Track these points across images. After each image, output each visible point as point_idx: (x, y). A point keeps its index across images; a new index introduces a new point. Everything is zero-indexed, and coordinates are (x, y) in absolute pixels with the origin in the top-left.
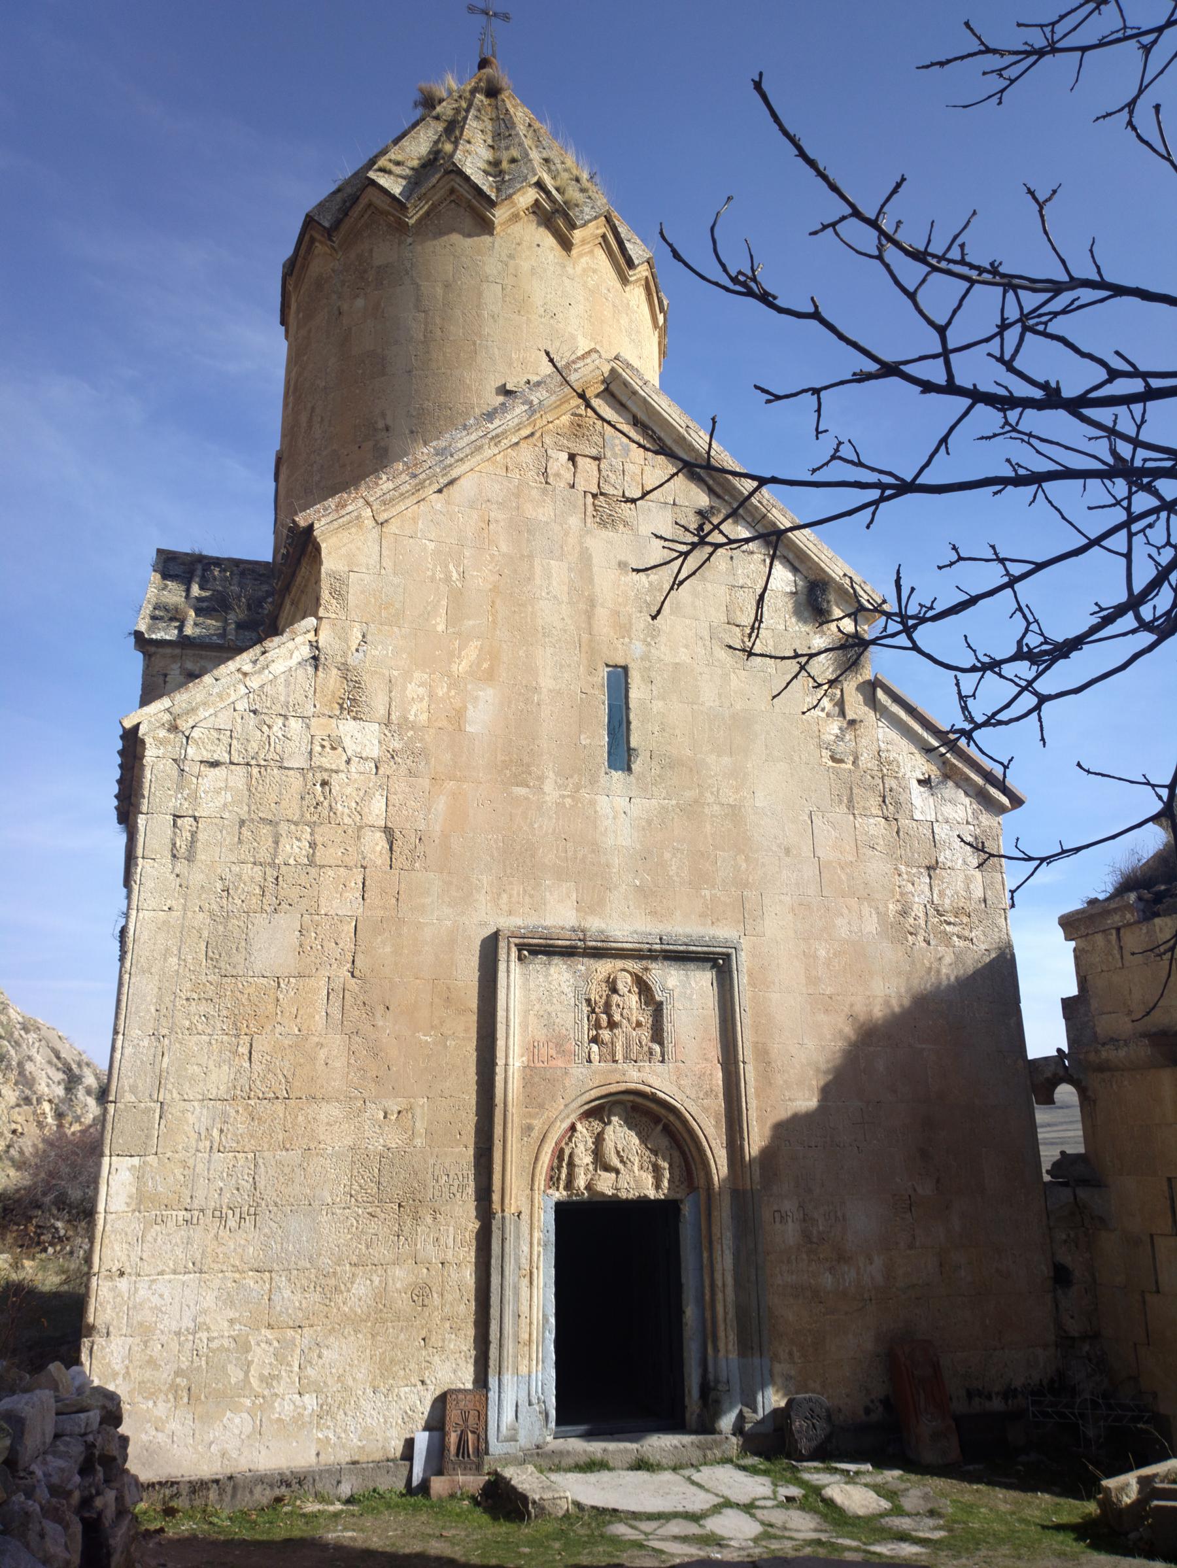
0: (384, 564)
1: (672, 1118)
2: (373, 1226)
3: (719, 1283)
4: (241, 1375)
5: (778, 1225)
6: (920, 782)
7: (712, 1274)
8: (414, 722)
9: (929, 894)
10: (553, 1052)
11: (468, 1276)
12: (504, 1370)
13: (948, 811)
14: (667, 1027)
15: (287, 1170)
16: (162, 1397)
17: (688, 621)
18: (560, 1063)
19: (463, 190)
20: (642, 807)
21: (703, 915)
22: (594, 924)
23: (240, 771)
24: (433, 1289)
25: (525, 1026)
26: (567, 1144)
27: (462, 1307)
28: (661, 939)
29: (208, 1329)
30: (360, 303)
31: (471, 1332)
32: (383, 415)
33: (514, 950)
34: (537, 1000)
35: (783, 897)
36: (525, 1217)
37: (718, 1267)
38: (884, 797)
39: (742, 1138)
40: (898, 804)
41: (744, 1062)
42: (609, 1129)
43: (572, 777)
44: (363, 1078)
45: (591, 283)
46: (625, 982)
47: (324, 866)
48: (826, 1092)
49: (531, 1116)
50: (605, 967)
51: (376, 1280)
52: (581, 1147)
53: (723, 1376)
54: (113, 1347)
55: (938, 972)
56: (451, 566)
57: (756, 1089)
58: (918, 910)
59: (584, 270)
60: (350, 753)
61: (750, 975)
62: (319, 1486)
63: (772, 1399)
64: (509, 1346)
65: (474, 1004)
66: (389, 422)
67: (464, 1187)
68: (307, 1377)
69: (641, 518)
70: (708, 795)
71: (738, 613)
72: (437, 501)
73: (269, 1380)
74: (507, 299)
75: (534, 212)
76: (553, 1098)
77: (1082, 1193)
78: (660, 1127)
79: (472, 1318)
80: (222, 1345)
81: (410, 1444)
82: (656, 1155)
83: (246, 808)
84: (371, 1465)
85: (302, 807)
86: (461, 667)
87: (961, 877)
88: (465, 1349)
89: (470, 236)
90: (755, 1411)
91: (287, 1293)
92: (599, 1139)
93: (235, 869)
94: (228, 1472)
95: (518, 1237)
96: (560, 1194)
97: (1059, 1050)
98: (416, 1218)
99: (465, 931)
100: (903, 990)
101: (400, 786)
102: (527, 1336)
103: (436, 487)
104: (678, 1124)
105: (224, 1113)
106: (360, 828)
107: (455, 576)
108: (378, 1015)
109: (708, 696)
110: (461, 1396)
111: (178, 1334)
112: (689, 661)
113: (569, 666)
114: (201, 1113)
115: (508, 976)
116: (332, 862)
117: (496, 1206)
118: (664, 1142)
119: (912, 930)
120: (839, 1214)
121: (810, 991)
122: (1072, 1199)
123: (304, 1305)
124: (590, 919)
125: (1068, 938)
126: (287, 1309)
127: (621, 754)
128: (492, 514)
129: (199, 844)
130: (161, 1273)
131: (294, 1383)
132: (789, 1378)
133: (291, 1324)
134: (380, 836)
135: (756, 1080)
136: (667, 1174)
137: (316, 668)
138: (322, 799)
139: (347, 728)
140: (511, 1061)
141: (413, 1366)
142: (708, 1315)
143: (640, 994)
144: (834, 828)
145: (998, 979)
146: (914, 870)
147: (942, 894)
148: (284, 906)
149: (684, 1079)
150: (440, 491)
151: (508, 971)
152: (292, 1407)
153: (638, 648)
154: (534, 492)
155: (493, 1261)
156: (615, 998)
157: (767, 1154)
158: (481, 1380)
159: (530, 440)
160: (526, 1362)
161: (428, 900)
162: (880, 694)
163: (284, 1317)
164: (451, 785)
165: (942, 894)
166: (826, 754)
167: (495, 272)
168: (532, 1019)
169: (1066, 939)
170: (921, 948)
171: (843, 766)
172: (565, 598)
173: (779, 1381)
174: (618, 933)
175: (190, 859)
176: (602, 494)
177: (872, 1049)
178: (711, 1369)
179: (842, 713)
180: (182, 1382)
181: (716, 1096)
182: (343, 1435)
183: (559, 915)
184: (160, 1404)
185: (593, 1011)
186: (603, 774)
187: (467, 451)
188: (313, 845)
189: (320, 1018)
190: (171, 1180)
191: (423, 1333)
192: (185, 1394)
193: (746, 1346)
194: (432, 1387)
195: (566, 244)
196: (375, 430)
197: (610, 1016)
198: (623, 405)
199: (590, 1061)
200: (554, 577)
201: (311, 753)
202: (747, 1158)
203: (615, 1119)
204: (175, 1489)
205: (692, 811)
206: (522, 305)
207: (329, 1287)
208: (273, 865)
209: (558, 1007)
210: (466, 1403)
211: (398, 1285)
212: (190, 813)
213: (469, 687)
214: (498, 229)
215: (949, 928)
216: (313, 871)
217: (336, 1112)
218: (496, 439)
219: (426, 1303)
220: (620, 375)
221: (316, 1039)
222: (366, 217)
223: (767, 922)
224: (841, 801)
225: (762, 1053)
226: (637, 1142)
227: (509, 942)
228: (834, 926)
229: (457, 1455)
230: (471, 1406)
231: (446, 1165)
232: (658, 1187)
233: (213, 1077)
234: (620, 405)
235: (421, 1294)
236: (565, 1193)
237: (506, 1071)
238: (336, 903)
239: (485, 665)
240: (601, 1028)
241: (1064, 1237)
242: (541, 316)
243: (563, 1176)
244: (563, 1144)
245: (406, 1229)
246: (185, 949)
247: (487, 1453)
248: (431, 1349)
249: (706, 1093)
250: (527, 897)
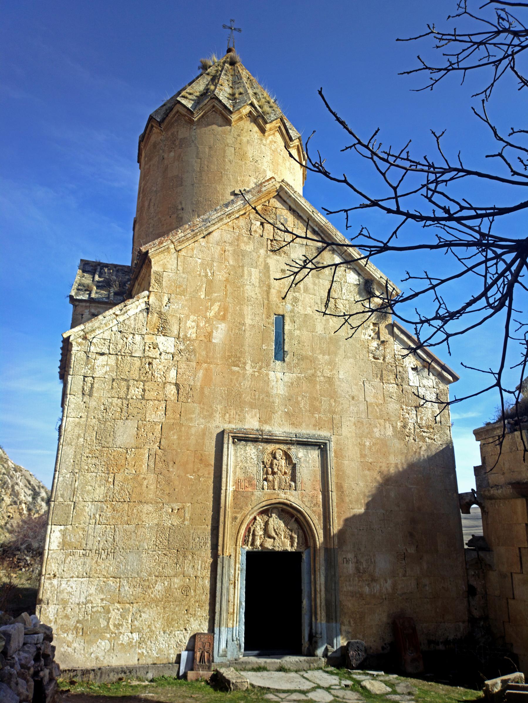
0: (179, 269)
1: (299, 515)
2: (166, 560)
3: (318, 589)
4: (106, 624)
5: (345, 564)
6: (412, 369)
7: (315, 585)
8: (190, 337)
9: (415, 419)
10: (247, 485)
11: (207, 583)
12: (222, 625)
13: (425, 382)
14: (298, 474)
15: (128, 533)
16: (71, 632)
17: (311, 296)
18: (250, 489)
19: (219, 106)
20: (288, 377)
21: (315, 426)
22: (267, 428)
23: (113, 357)
24: (191, 588)
25: (235, 473)
26: (252, 526)
27: (204, 596)
28: (296, 435)
29: (92, 603)
30: (172, 154)
31: (207, 608)
32: (181, 203)
33: (231, 438)
34: (240, 461)
35: (350, 418)
36: (233, 557)
37: (318, 582)
38: (396, 375)
39: (330, 525)
40: (402, 379)
41: (332, 491)
42: (271, 520)
43: (258, 363)
44: (163, 493)
45: (273, 148)
46: (279, 454)
47: (148, 400)
48: (368, 505)
49: (236, 512)
50: (270, 447)
51: (166, 583)
52: (258, 527)
53: (319, 631)
54: (50, 609)
55: (420, 453)
56: (208, 270)
57: (337, 503)
58: (410, 425)
59: (271, 142)
60: (161, 350)
61: (335, 452)
62: (139, 674)
63: (341, 642)
64: (224, 615)
65: (212, 462)
66: (183, 206)
67: (205, 543)
68: (135, 625)
69: (292, 250)
70: (318, 372)
71: (334, 293)
72: (203, 242)
73: (117, 626)
74: (236, 154)
75: (249, 116)
76: (247, 505)
77: (481, 554)
78: (294, 519)
79: (208, 601)
80: (98, 610)
81: (179, 656)
82: (292, 532)
83: (115, 374)
84: (162, 665)
85: (139, 374)
86: (211, 314)
87: (430, 411)
88: (204, 615)
89: (221, 126)
90: (333, 647)
91: (127, 588)
92: (266, 524)
93: (110, 400)
94: (99, 666)
95: (229, 566)
96: (249, 548)
97: (472, 490)
98: (185, 556)
99: (209, 430)
100: (403, 461)
101: (183, 365)
102: (232, 611)
103: (202, 236)
104: (302, 518)
105: (102, 507)
106: (165, 383)
107: (209, 274)
108: (170, 466)
110: (202, 636)
111: (78, 604)
112: (311, 313)
113: (258, 314)
114: (91, 507)
115: (228, 450)
116: (152, 398)
117: (220, 552)
118: (296, 526)
119: (408, 434)
120: (373, 560)
121: (362, 460)
122: (477, 556)
123: (134, 593)
124: (265, 426)
125: (477, 440)
126: (127, 595)
127: (280, 353)
128: (227, 248)
129: (94, 389)
130: (72, 577)
131: (128, 628)
132: (348, 633)
133: (128, 601)
134: (173, 387)
135: (337, 499)
136: (296, 540)
137: (148, 313)
138: (148, 370)
139: (160, 339)
140: (228, 488)
141: (181, 622)
142: (313, 604)
143: (286, 460)
144: (374, 388)
145: (446, 457)
146: (409, 408)
147: (421, 419)
148: (131, 417)
149: (304, 498)
150: (204, 237)
151: (228, 448)
152: (128, 638)
153: (289, 307)
154: (245, 239)
155: (218, 577)
156: (275, 461)
157: (341, 532)
158: (211, 629)
159: (244, 216)
160: (231, 622)
161: (194, 416)
162: (395, 329)
163: (125, 598)
164: (205, 365)
165: (421, 419)
166: (371, 355)
167: (231, 142)
168: (238, 469)
169: (477, 440)
170: (412, 443)
171: (378, 361)
172: (257, 285)
173: (344, 633)
174: (277, 432)
175: (90, 395)
176: (275, 240)
177: (389, 487)
178: (314, 627)
179: (379, 338)
180: (80, 626)
181: (319, 506)
182: (150, 652)
183: (252, 423)
184: (70, 635)
185: (265, 467)
186: (272, 362)
187: (217, 220)
188: (144, 390)
189: (145, 467)
190: (77, 536)
191: (186, 607)
192: (81, 631)
193: (329, 619)
194: (189, 632)
195: (263, 131)
196: (177, 209)
197: (272, 469)
198: (285, 201)
199: (263, 489)
200: (254, 275)
201: (144, 350)
202: (332, 534)
203: (274, 515)
204: (75, 673)
205: (311, 379)
206: (243, 156)
207: (146, 586)
208: (126, 399)
209: (250, 464)
210: (204, 639)
211: (176, 586)
212: (91, 375)
213: (214, 323)
214: (233, 124)
215: (424, 434)
216: (144, 402)
217: (150, 509)
218: (229, 216)
219: (188, 594)
220: (284, 189)
221: (143, 476)
222: (176, 117)
223: (343, 429)
224: (377, 377)
225: (340, 487)
226: (283, 525)
227: (229, 435)
228: (373, 432)
229: (200, 662)
230: (206, 640)
231: (199, 533)
232: (292, 546)
233: (97, 491)
234: (284, 202)
235: (185, 590)
236: (251, 547)
237: (226, 492)
238: (153, 416)
239: (222, 313)
240: (268, 474)
241: (473, 573)
242: (251, 162)
243: (250, 540)
244: (250, 526)
245: (180, 561)
246: (87, 435)
247: (213, 662)
248: (189, 615)
249: (314, 505)
250: (237, 416)
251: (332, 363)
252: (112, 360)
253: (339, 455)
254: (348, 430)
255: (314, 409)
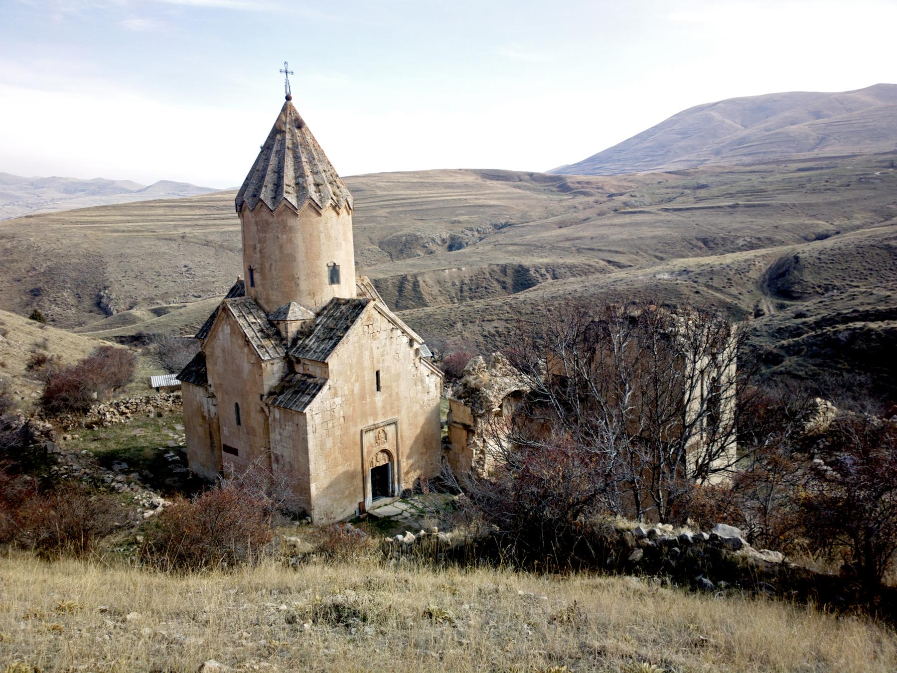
20: (383, 397)
34: (369, 438)
109: (393, 372)
127: (378, 389)
139: (336, 399)
195: (338, 214)
200: (367, 354)
205: (390, 396)
206: (329, 238)
207: (343, 493)
235: (355, 490)
251: (398, 385)
252: (320, 415)
253: (401, 424)
254: (404, 412)
255: (392, 408)
